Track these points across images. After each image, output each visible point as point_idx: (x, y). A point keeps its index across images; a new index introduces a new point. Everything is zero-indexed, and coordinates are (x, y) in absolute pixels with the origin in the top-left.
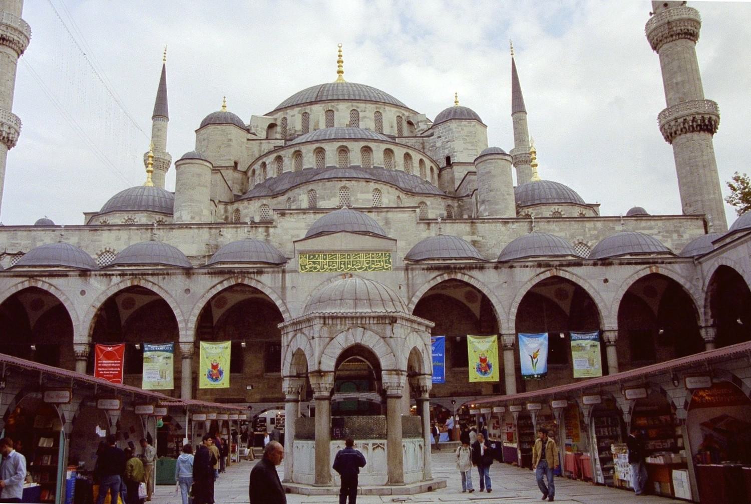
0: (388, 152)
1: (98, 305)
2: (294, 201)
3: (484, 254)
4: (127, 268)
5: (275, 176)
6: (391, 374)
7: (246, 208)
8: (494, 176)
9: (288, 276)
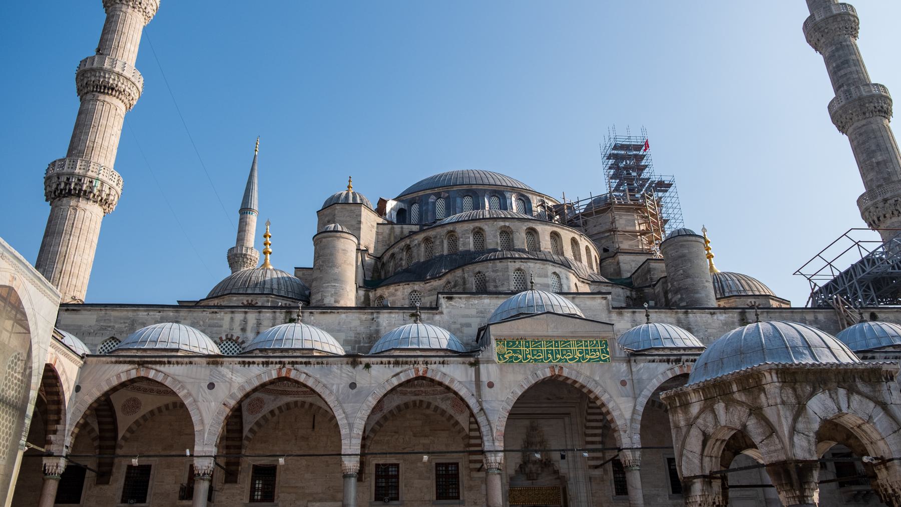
0: (555, 236)
1: (233, 403)
2: (455, 286)
4: (271, 354)
5: (422, 260)
7: (393, 295)
8: (690, 260)
9: (481, 366)
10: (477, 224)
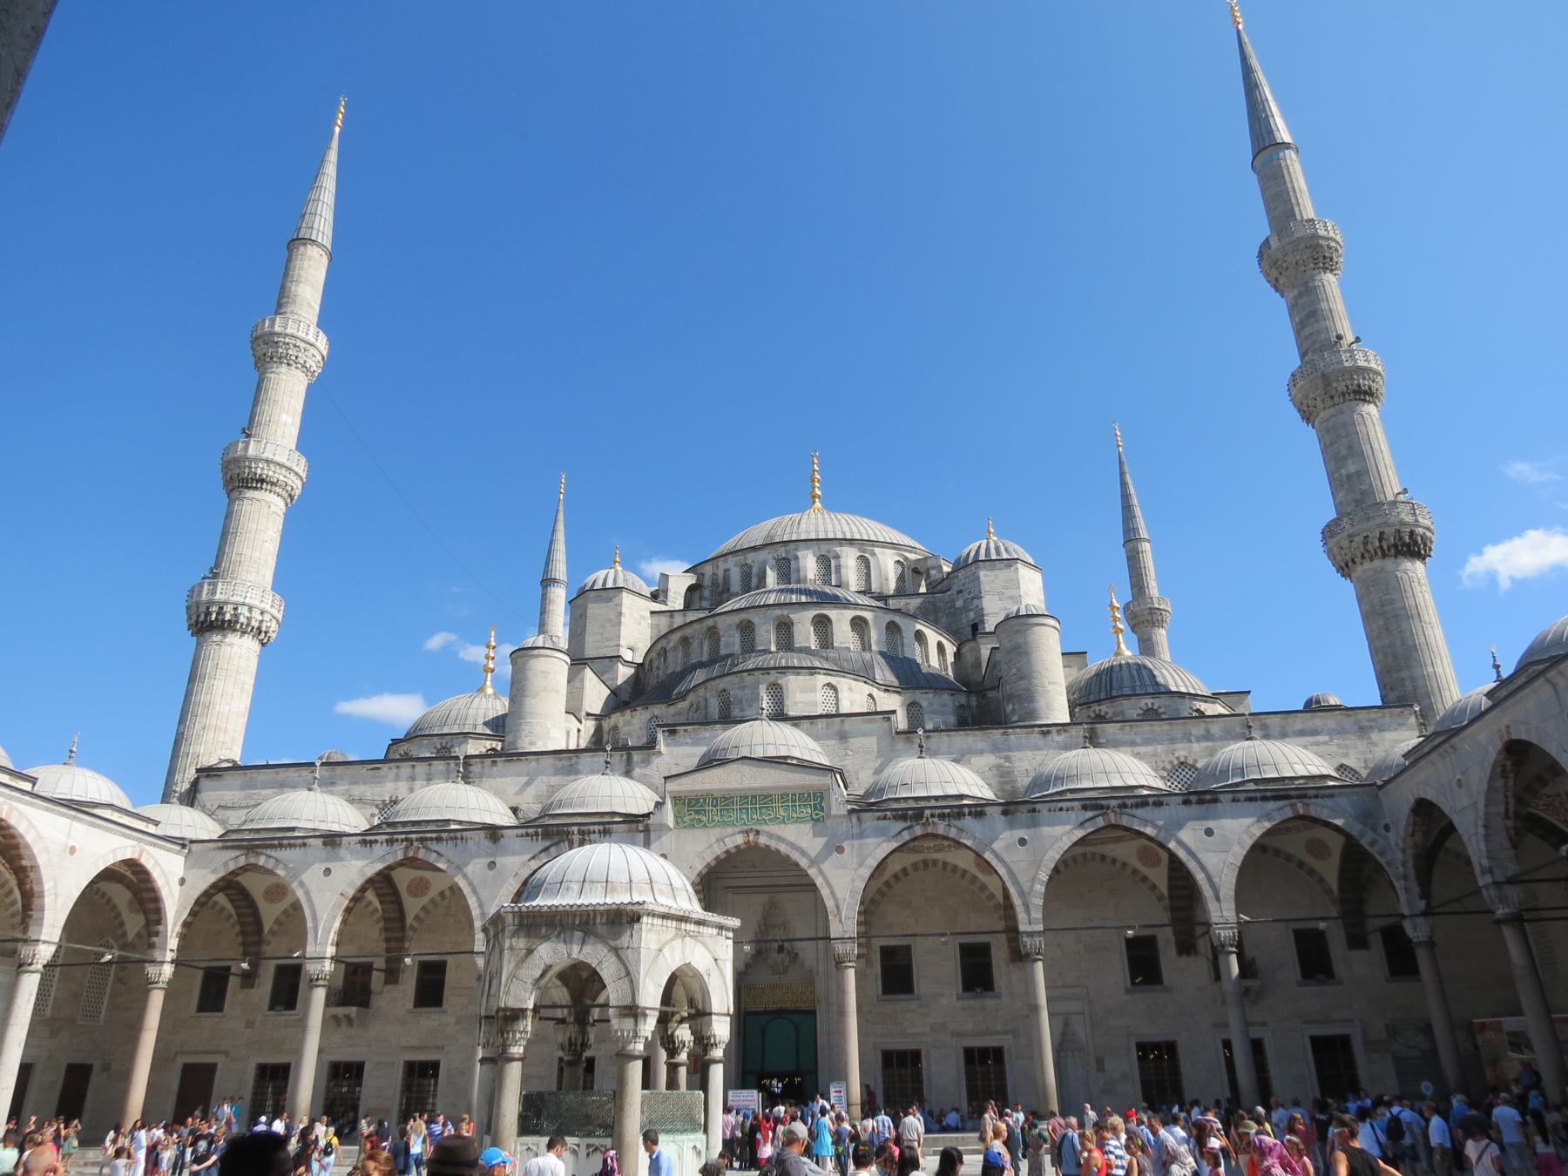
1: (351, 892)
3: (1008, 787)
6: (625, 1016)
7: (628, 723)
10: (743, 616)
